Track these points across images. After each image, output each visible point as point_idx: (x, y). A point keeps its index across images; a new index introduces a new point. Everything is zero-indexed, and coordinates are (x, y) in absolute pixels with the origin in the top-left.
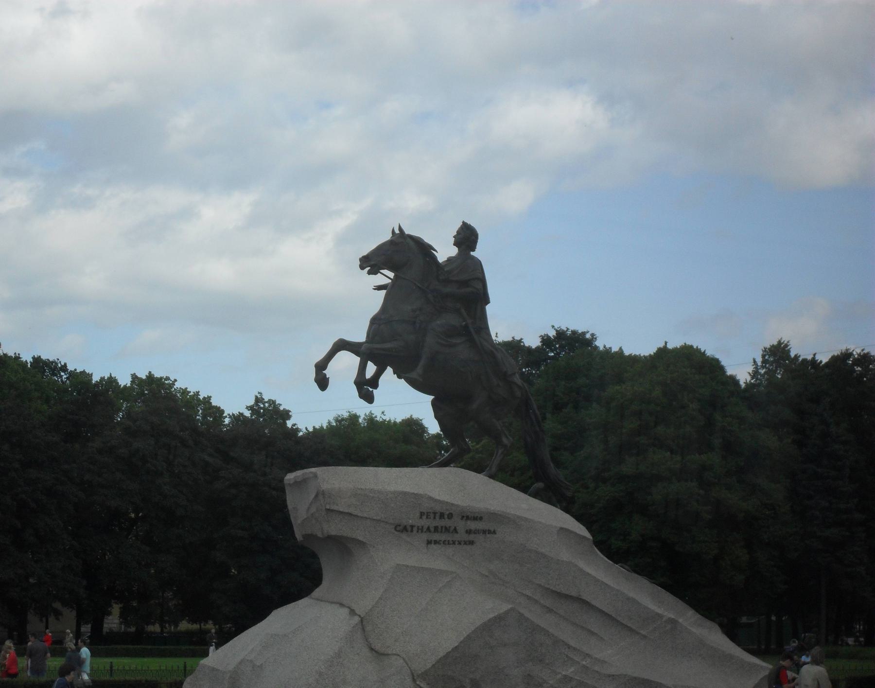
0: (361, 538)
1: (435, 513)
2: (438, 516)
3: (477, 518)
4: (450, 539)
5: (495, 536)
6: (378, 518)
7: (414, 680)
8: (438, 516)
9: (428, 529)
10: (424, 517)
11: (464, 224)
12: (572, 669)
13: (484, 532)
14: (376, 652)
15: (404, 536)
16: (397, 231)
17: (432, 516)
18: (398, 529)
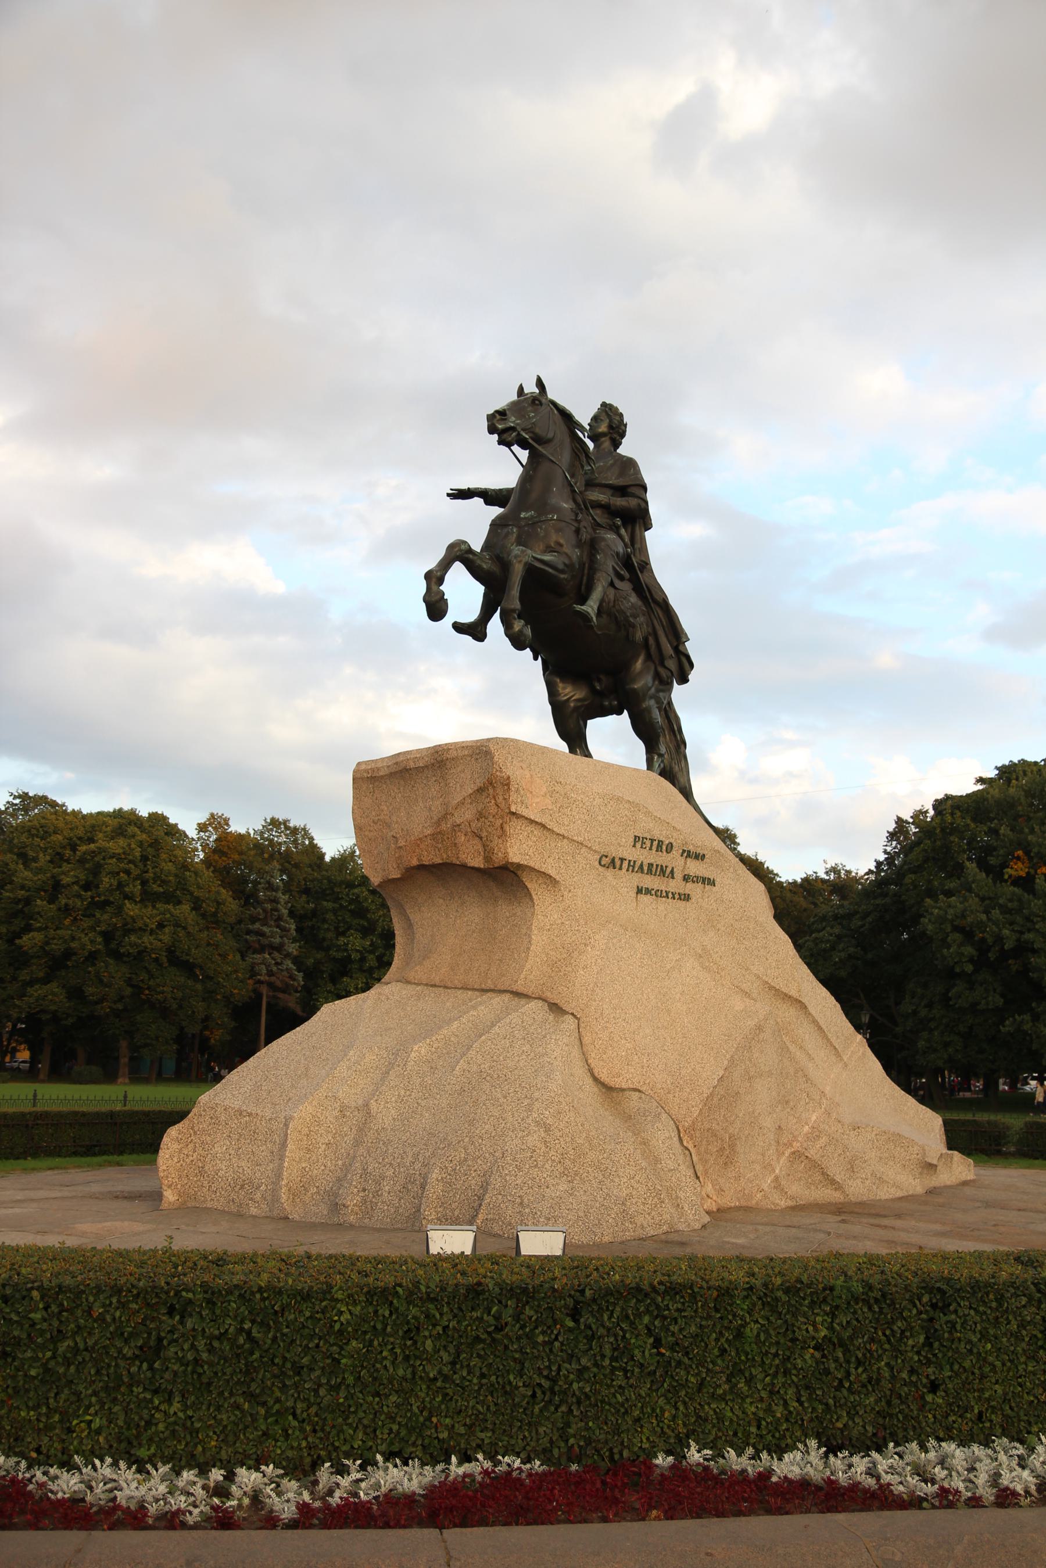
0: (552, 872)
1: (652, 840)
2: (655, 843)
3: (699, 857)
4: (663, 888)
5: (714, 889)
6: (580, 839)
7: (681, 1140)
8: (655, 843)
9: (641, 866)
10: (638, 845)
11: (604, 404)
12: (814, 1118)
14: (603, 1085)
15: (609, 873)
16: (531, 388)
17: (648, 843)
18: (604, 861)
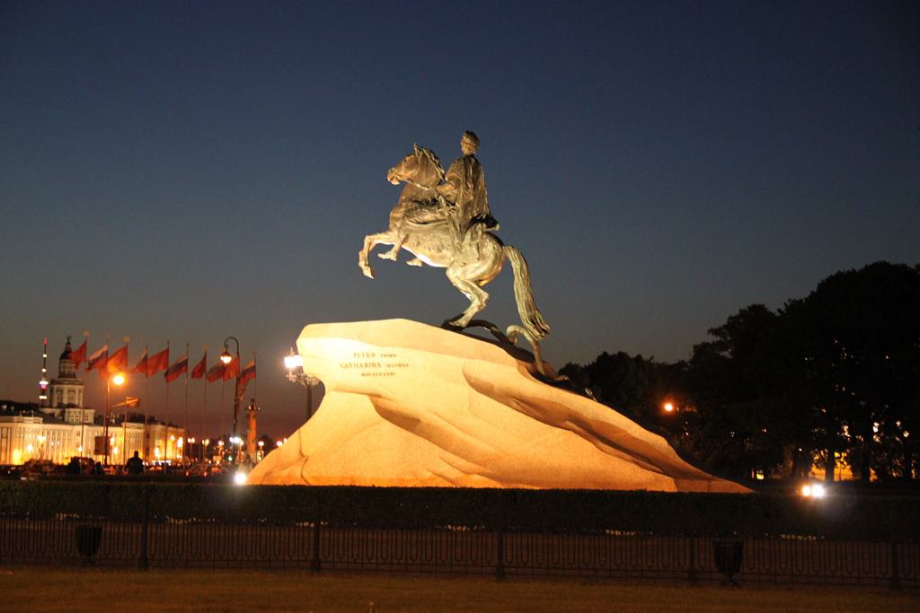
9: (361, 365)
13: (400, 365)
